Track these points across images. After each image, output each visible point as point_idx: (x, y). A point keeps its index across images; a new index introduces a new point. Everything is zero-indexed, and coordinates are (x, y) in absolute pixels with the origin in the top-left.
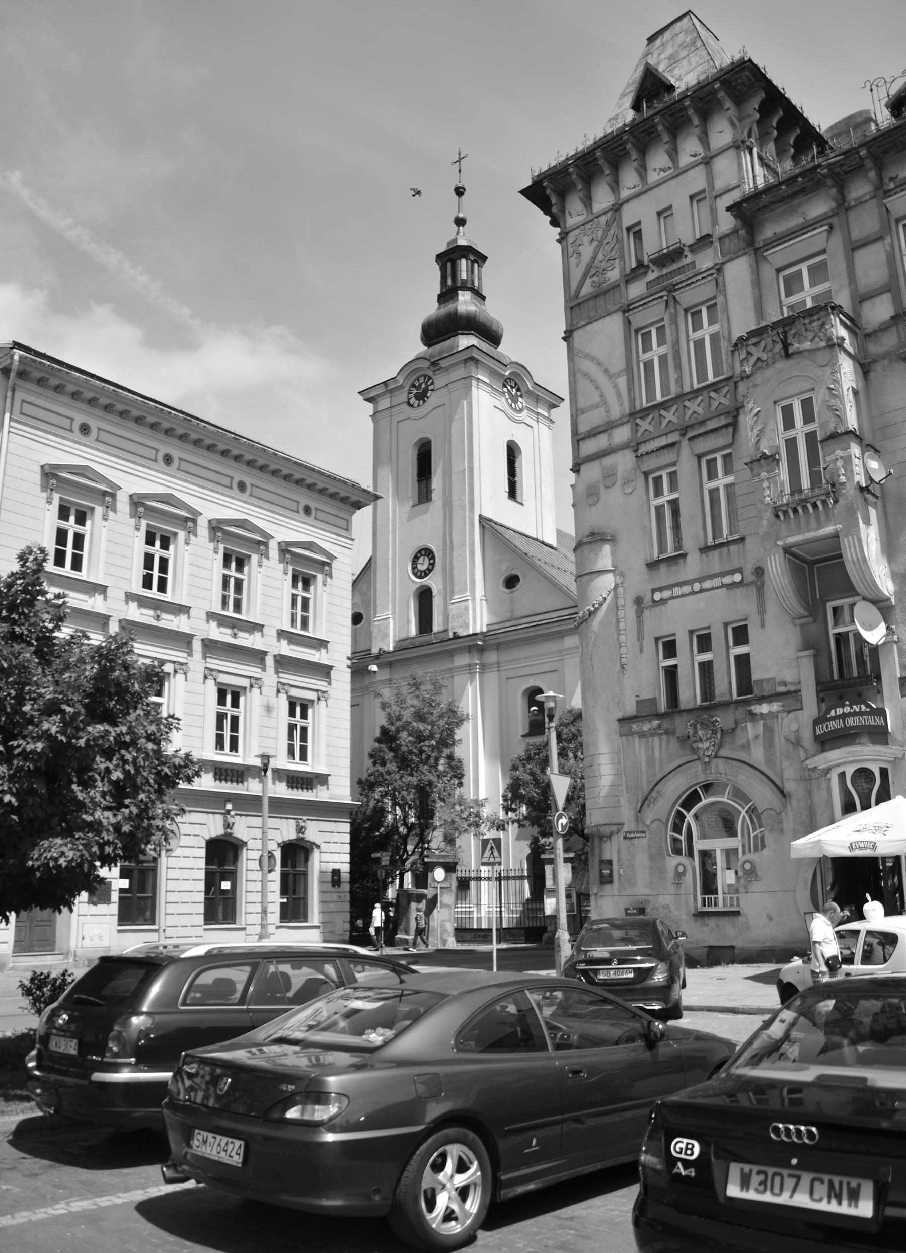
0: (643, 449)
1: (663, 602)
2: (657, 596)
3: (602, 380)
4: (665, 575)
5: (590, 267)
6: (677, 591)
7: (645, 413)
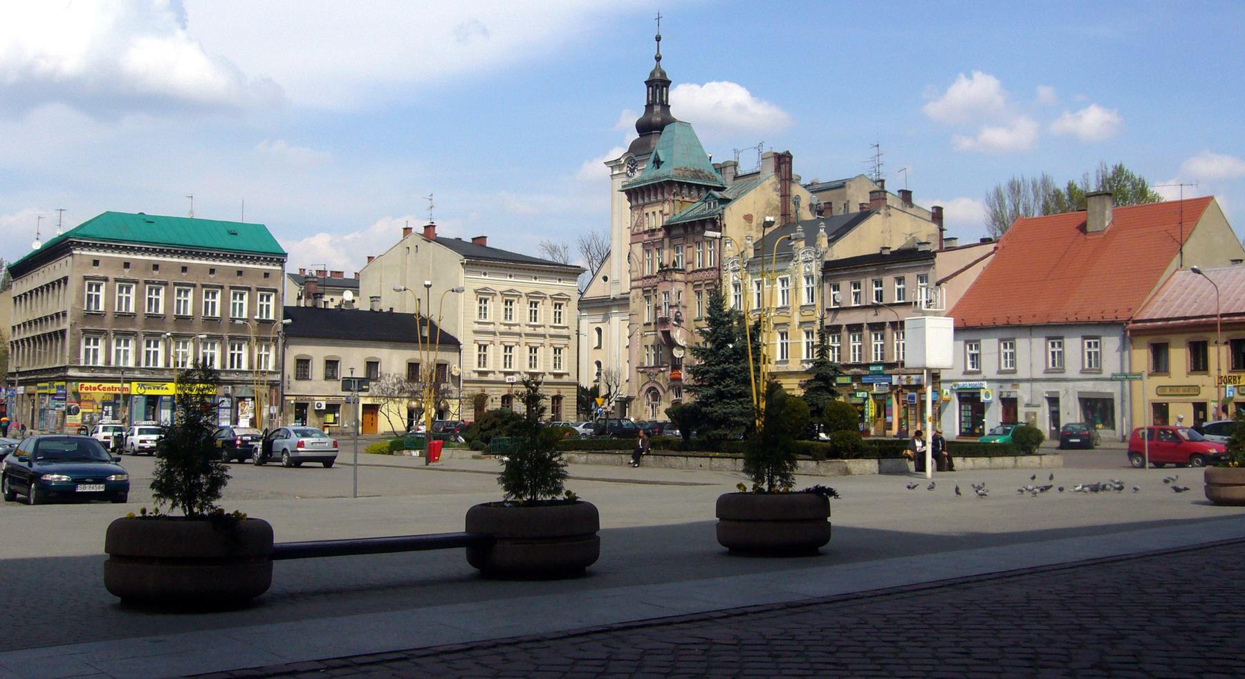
0: (645, 289)
1: (646, 336)
2: (646, 334)
3: (637, 263)
4: (648, 328)
5: (636, 223)
6: (649, 333)
7: (645, 278)
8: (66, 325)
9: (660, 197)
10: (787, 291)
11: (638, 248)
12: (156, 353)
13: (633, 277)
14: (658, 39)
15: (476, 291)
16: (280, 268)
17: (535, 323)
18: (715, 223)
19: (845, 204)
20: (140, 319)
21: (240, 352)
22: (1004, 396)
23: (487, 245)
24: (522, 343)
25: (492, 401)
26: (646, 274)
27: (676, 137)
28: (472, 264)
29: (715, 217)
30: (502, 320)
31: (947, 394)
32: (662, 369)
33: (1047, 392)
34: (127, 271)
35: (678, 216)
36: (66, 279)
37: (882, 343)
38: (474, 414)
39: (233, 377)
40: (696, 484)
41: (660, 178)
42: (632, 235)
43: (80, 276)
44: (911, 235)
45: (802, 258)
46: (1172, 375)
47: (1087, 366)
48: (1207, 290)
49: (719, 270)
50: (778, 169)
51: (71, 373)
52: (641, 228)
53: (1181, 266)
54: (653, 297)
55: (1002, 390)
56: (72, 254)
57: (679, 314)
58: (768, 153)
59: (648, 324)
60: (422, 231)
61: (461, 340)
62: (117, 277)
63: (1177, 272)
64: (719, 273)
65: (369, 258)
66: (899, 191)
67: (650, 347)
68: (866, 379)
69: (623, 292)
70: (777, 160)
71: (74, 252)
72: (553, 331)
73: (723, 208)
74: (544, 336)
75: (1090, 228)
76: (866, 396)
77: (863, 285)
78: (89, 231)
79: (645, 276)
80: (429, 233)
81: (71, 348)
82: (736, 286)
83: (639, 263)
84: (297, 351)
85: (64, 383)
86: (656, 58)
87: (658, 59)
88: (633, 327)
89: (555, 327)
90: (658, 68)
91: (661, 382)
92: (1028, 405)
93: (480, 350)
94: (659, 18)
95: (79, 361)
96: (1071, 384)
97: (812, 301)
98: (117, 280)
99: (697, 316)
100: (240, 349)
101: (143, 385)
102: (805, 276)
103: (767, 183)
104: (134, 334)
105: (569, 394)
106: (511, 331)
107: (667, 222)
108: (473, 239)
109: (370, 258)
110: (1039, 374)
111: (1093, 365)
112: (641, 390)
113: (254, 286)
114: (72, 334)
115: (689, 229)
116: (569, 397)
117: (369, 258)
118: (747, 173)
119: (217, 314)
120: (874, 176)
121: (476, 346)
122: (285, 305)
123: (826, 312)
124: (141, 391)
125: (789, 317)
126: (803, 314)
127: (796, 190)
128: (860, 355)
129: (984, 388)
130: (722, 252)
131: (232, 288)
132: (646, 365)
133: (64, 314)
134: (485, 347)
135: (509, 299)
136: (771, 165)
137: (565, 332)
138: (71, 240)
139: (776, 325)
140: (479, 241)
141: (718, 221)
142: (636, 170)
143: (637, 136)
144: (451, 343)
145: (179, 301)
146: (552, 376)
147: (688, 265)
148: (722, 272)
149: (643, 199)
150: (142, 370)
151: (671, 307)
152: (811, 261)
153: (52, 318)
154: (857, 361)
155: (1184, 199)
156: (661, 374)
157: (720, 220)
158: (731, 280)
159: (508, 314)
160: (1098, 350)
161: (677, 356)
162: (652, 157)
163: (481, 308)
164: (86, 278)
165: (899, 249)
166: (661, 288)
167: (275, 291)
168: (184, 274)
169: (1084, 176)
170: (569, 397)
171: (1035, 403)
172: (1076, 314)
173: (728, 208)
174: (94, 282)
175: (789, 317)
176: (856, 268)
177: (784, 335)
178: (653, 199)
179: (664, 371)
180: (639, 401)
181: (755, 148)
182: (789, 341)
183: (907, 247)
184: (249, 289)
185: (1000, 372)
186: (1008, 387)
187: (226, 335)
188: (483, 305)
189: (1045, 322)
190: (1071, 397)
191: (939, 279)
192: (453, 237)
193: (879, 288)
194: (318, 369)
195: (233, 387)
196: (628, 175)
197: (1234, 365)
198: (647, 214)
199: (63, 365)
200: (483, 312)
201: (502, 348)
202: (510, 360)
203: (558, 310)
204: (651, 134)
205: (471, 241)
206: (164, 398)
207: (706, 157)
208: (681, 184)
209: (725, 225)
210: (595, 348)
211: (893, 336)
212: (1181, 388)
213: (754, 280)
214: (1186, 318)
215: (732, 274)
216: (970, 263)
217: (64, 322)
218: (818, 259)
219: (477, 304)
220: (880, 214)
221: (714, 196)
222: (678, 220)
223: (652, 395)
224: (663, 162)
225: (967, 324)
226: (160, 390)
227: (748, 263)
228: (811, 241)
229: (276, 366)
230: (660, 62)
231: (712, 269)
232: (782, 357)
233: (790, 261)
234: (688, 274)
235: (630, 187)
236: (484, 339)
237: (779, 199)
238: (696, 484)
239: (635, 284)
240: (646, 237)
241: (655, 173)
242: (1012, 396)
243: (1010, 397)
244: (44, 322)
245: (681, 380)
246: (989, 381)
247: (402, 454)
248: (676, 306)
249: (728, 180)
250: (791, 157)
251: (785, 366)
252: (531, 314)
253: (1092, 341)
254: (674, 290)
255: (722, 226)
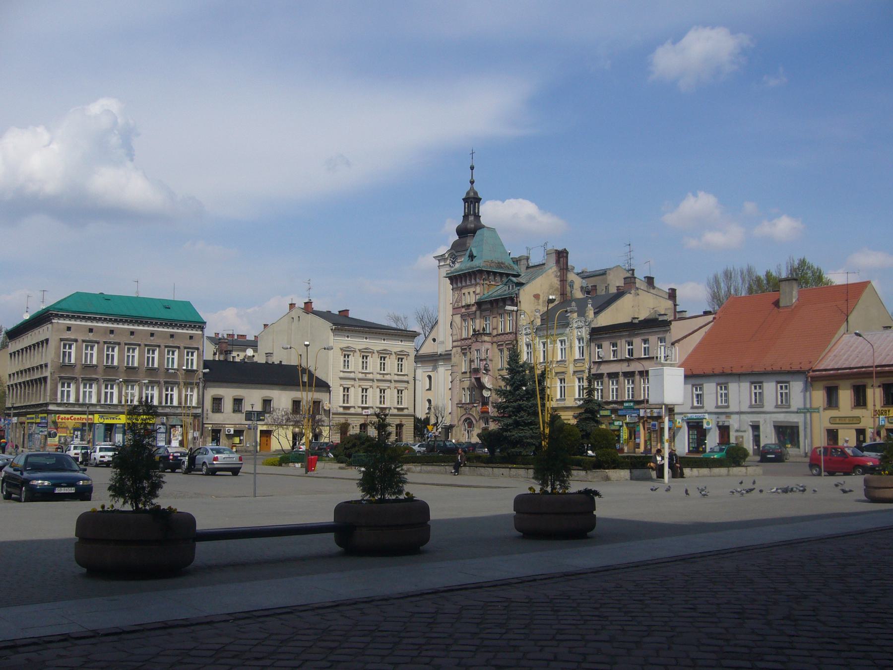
0: (463, 347)
1: (463, 381)
2: (463, 379)
4: (464, 376)
5: (456, 300)
6: (466, 379)
7: (463, 340)
8: (47, 373)
9: (473, 282)
10: (565, 349)
11: (458, 318)
12: (112, 393)
13: (454, 339)
14: (472, 168)
15: (341, 349)
16: (201, 333)
17: (384, 372)
18: (513, 300)
19: (606, 287)
20: (100, 369)
21: (172, 393)
22: (720, 424)
23: (350, 316)
24: (375, 387)
25: (353, 427)
26: (464, 336)
27: (485, 238)
28: (338, 330)
29: (513, 296)
30: (360, 370)
31: (679, 423)
32: (475, 405)
33: (751, 422)
34: (91, 334)
35: (486, 295)
36: (47, 340)
37: (633, 386)
38: (340, 437)
39: (167, 410)
40: (499, 487)
41: (473, 268)
42: (454, 309)
43: (58, 338)
44: (653, 309)
45: (575, 325)
46: (840, 410)
47: (779, 403)
48: (866, 348)
49: (516, 334)
50: (558, 262)
51: (51, 408)
52: (460, 304)
53: (847, 331)
54: (468, 353)
55: (718, 420)
56: (52, 322)
57: (487, 366)
58: (551, 250)
59: (465, 373)
60: (303, 306)
61: (330, 384)
62: (84, 339)
63: (844, 335)
64: (516, 336)
65: (265, 325)
66: (645, 277)
67: (466, 389)
68: (621, 412)
69: (447, 350)
70: (557, 255)
71: (53, 321)
72: (396, 378)
73: (519, 290)
74: (390, 381)
75: (782, 304)
76: (621, 424)
77: (619, 345)
78: (64, 306)
79: (462, 338)
80: (308, 308)
81: (51, 390)
82: (528, 345)
83: (459, 329)
84: (213, 392)
85: (46, 415)
86: (471, 182)
87: (472, 182)
88: (454, 375)
89: (398, 375)
90: (472, 189)
91: (474, 414)
92: (737, 431)
93: (344, 391)
94: (472, 153)
95: (56, 399)
96: (768, 416)
97: (583, 356)
98: (84, 341)
99: (500, 367)
100: (172, 390)
101: (102, 416)
102: (577, 339)
103: (550, 271)
104: (96, 380)
105: (407, 423)
106: (367, 377)
107: (479, 299)
108: (340, 312)
109: (265, 326)
110: (745, 408)
111: (784, 402)
112: (460, 420)
113: (182, 345)
114: (52, 379)
115: (494, 305)
116: (409, 425)
117: (265, 325)
118: (536, 264)
119: (156, 365)
120: (627, 267)
121: (342, 389)
122: (205, 359)
123: (592, 364)
124: (101, 421)
125: (566, 367)
126: (576, 365)
127: (571, 276)
128: (617, 395)
129: (706, 419)
130: (518, 322)
131: (166, 347)
132: (463, 402)
133: (46, 366)
134: (348, 389)
135: (365, 354)
136: (553, 259)
137: (405, 378)
138: (51, 312)
139: (557, 373)
140: (344, 313)
141: (515, 299)
142: (456, 262)
143: (457, 238)
144: (323, 386)
145: (128, 356)
146: (396, 410)
147: (494, 331)
148: (518, 335)
149: (461, 282)
150: (102, 406)
151: (481, 360)
152: (582, 327)
153: (37, 368)
154: (615, 399)
155: (849, 283)
156: (474, 408)
157: (517, 298)
158: (525, 341)
159: (364, 365)
160: (787, 391)
161: (486, 396)
162: (468, 253)
163: (345, 361)
164: (61, 340)
165: (645, 319)
166: (474, 347)
167: (198, 349)
168: (132, 337)
169: (777, 266)
170: (409, 425)
171: (742, 429)
172: (772, 365)
173: (522, 290)
174: (67, 343)
175: (566, 367)
176: (614, 332)
177: (562, 380)
178: (468, 283)
179: (476, 407)
180: (458, 428)
181: (541, 246)
182: (566, 385)
183: (651, 317)
184: (179, 348)
185: (717, 407)
186: (723, 418)
187: (162, 381)
188: (346, 359)
189: (749, 371)
190: (768, 425)
191: (673, 340)
192: (325, 311)
193: (631, 347)
194: (228, 405)
195: (167, 418)
196: (450, 266)
197: (885, 402)
198: (464, 294)
199: (45, 402)
200: (346, 364)
201: (360, 389)
202: (366, 398)
203: (400, 363)
204: (467, 236)
205: (337, 313)
206: (118, 425)
207: (507, 253)
208: (488, 272)
209: (520, 302)
210: (427, 390)
211: (640, 381)
212: (847, 418)
213: (541, 341)
214: (850, 368)
215: (525, 337)
216: (695, 329)
217: (46, 371)
218: (587, 326)
219: (342, 358)
220: (631, 293)
221: (512, 281)
222: (486, 298)
223: (468, 424)
224: (475, 256)
225: (694, 373)
226: (115, 420)
227: (537, 329)
228: (582, 313)
229: (198, 403)
230: (474, 185)
231: (510, 333)
232: (561, 396)
233: (567, 327)
234: (494, 336)
235: (452, 275)
236: (347, 383)
237: (559, 283)
238: (499, 487)
239: (455, 344)
240: (463, 310)
241: (469, 264)
242: (726, 424)
243: (725, 425)
244: (32, 371)
245: (489, 412)
246: (709, 413)
247: (288, 466)
248: (485, 360)
249: (522, 270)
250: (567, 253)
251: (563, 402)
252: (381, 365)
253: (783, 385)
254: (483, 348)
255: (518, 302)
